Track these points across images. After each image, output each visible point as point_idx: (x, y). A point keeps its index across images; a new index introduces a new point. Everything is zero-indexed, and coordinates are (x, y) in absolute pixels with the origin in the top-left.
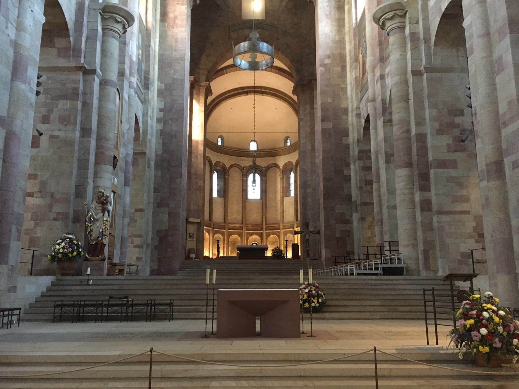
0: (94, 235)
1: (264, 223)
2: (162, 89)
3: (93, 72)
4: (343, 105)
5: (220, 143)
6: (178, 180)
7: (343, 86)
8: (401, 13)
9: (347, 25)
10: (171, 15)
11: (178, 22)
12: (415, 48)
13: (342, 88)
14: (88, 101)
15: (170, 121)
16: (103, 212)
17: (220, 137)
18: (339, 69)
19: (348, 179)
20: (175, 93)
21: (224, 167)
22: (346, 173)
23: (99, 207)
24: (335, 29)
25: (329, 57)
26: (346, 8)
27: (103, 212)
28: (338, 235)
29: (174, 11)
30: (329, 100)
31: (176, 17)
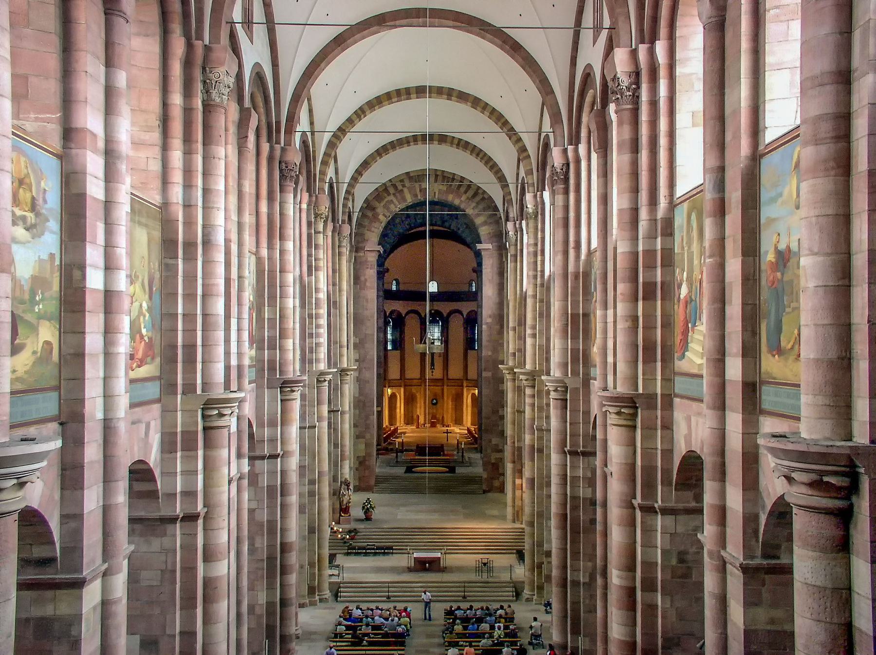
0: (344, 503)
1: (445, 378)
2: (356, 343)
3: (339, 411)
4: (500, 358)
5: (394, 288)
6: (371, 417)
7: (500, 342)
8: (511, 372)
9: (505, 291)
10: (362, 279)
11: (368, 284)
12: (519, 396)
13: (500, 343)
14: (336, 427)
15: (364, 370)
16: (348, 490)
17: (395, 280)
18: (498, 327)
19: (502, 418)
20: (367, 345)
21: (399, 314)
22: (501, 413)
23: (346, 487)
24: (496, 292)
25: (490, 317)
26: (505, 274)
27: (348, 490)
28: (493, 461)
29: (365, 275)
30: (490, 353)
31: (366, 280)
